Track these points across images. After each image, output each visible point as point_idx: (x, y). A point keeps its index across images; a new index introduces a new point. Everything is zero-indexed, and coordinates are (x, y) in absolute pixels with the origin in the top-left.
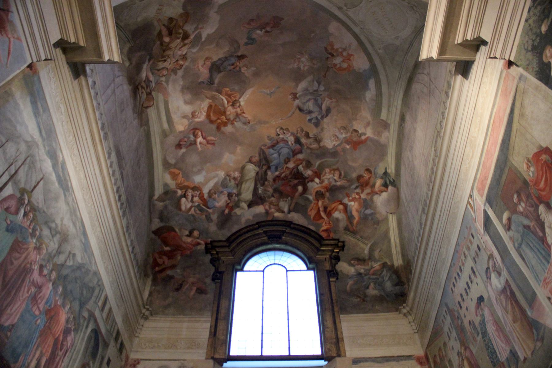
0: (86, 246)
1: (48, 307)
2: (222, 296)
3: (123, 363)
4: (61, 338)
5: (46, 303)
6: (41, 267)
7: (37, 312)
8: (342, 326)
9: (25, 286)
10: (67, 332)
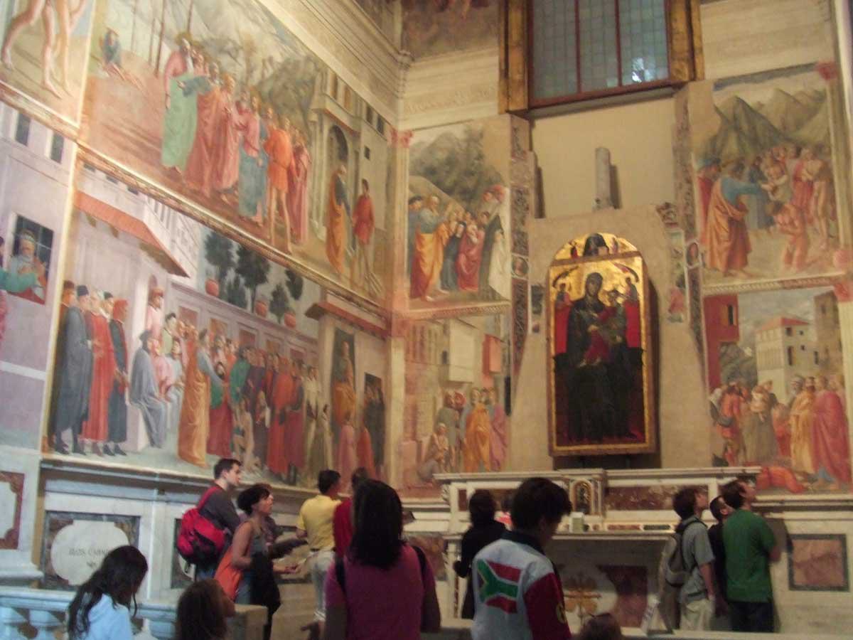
0: (283, 36)
2: (510, 5)
3: (390, 142)
4: (293, 163)
5: (261, 137)
6: (238, 104)
7: (255, 154)
8: (702, 23)
10: (297, 152)
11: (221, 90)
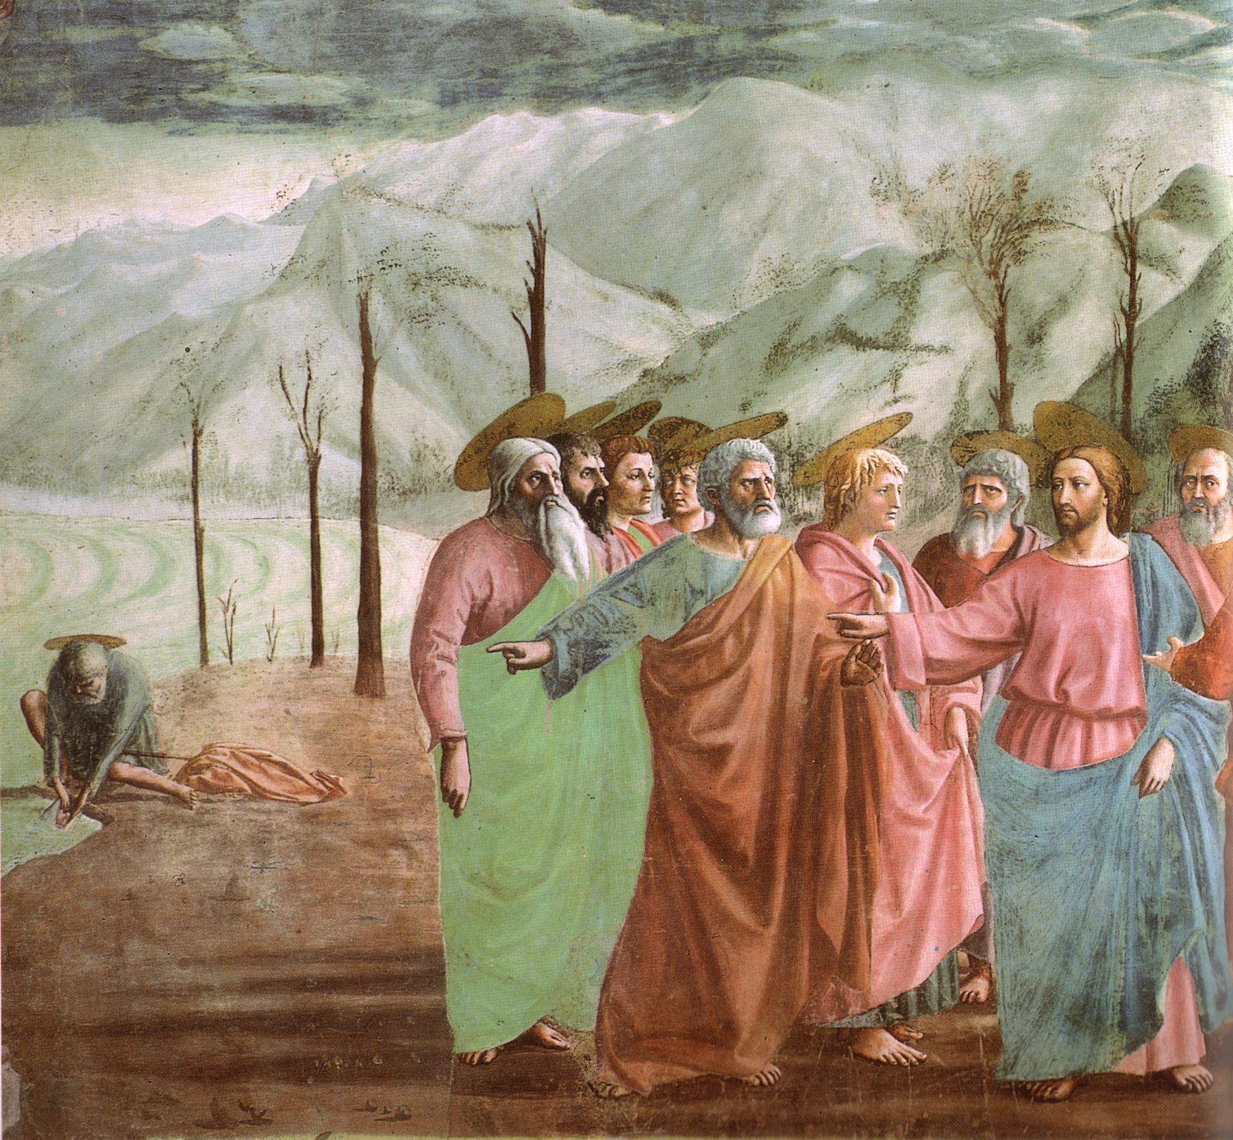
1: (1179, 643)
7: (1108, 741)
9: (901, 745)
11: (804, 547)
